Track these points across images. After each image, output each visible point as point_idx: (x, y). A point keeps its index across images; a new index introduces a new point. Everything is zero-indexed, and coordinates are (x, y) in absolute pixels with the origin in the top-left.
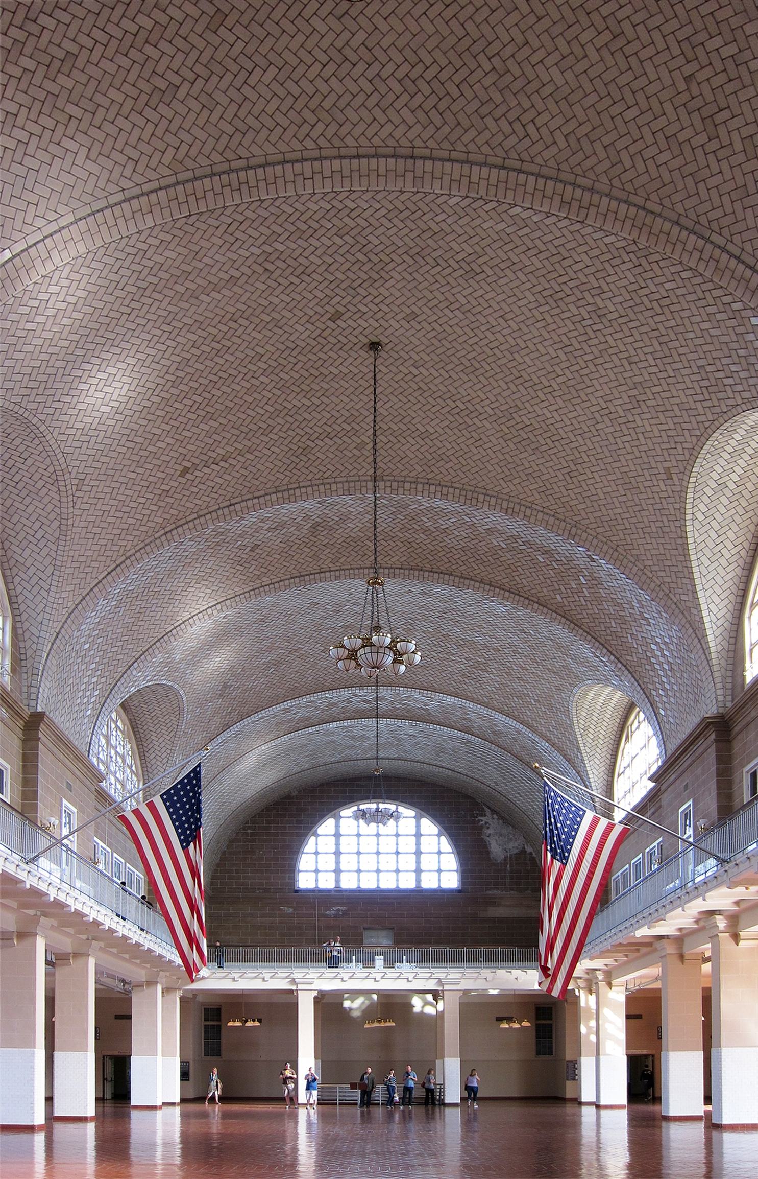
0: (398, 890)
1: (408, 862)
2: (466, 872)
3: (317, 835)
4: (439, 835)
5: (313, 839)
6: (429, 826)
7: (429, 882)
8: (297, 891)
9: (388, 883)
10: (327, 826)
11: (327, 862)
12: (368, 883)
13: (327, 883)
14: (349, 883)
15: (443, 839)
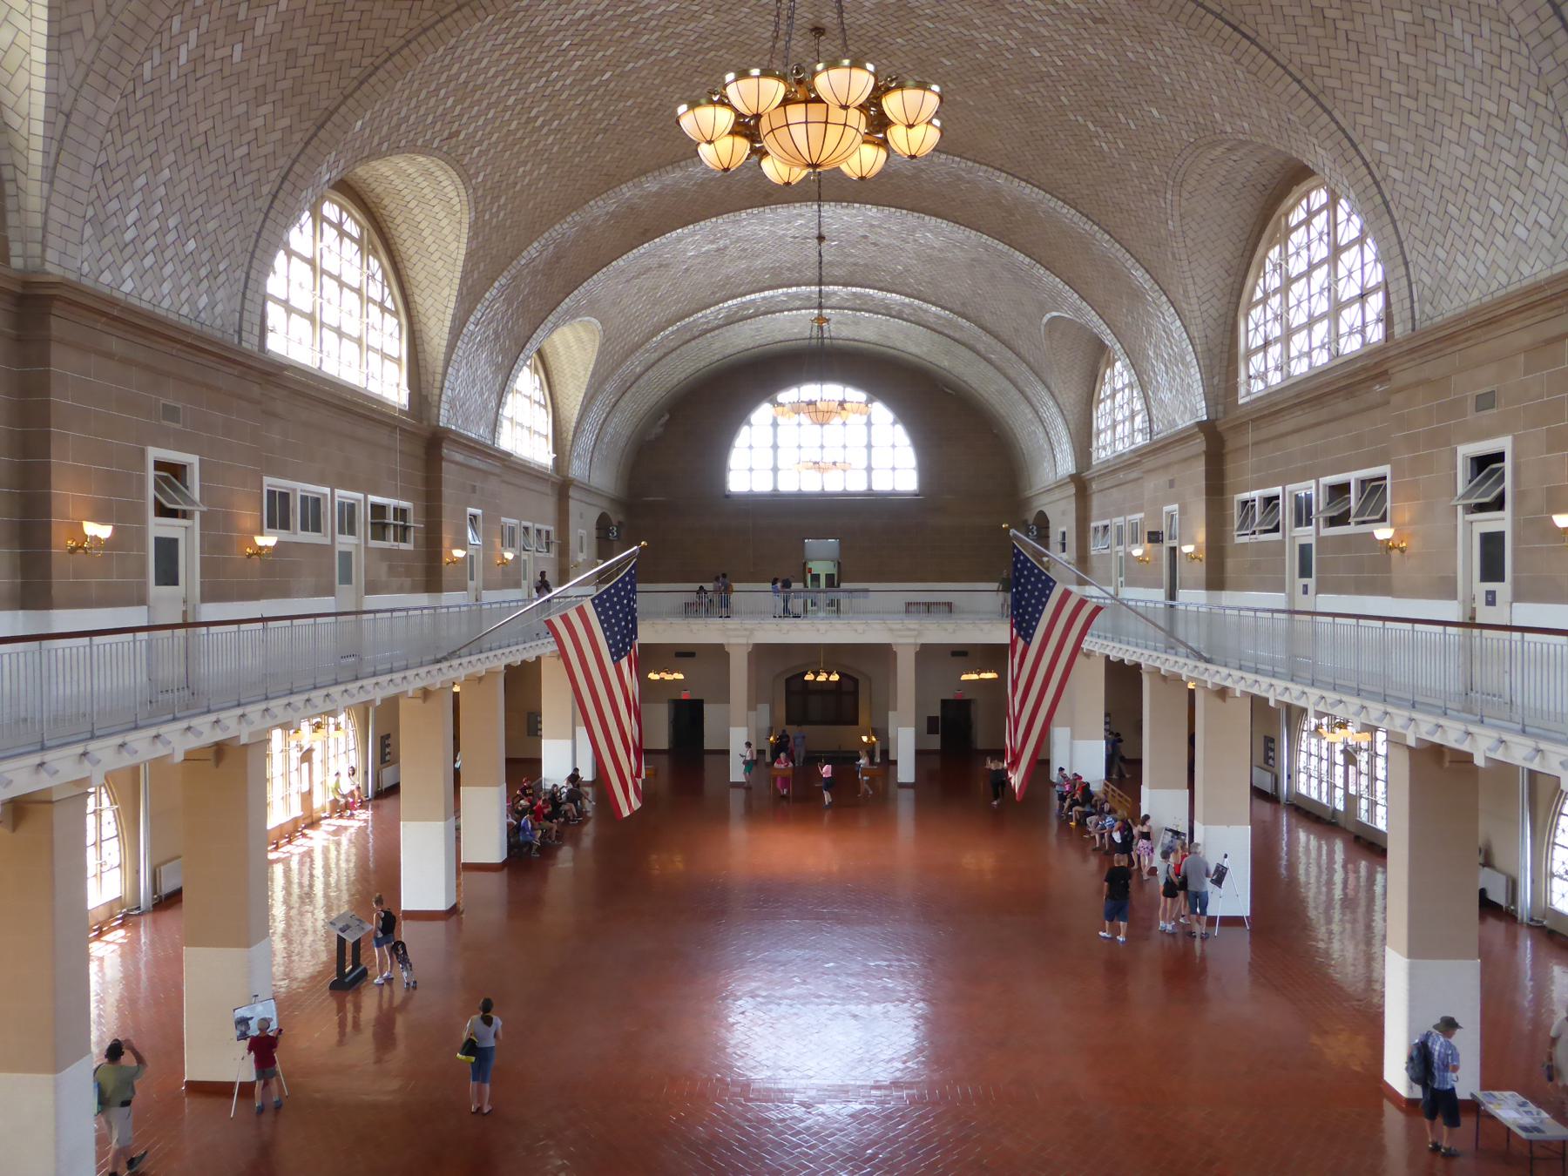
0: (846, 494)
1: (858, 458)
2: (925, 470)
3: (749, 424)
4: (894, 423)
5: (744, 431)
6: (882, 413)
7: (882, 484)
8: (728, 496)
9: (834, 483)
10: (763, 413)
11: (764, 459)
12: (811, 484)
13: (761, 484)
14: (788, 485)
15: (900, 430)
